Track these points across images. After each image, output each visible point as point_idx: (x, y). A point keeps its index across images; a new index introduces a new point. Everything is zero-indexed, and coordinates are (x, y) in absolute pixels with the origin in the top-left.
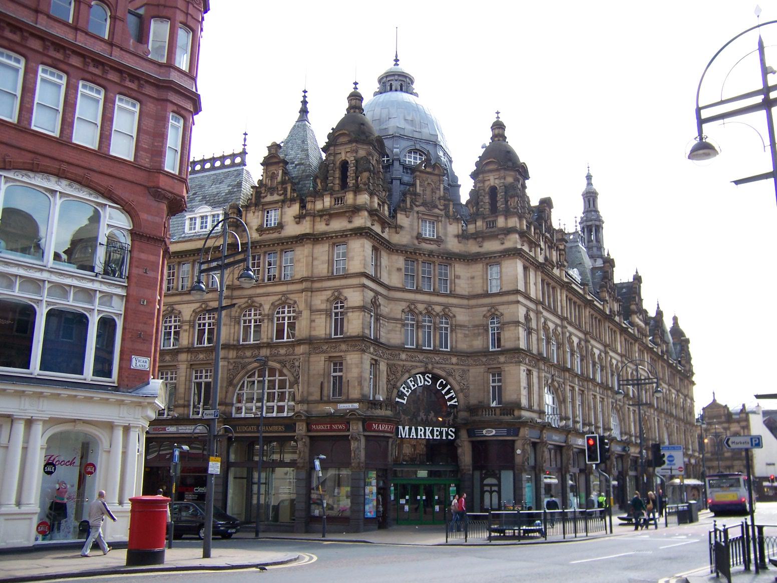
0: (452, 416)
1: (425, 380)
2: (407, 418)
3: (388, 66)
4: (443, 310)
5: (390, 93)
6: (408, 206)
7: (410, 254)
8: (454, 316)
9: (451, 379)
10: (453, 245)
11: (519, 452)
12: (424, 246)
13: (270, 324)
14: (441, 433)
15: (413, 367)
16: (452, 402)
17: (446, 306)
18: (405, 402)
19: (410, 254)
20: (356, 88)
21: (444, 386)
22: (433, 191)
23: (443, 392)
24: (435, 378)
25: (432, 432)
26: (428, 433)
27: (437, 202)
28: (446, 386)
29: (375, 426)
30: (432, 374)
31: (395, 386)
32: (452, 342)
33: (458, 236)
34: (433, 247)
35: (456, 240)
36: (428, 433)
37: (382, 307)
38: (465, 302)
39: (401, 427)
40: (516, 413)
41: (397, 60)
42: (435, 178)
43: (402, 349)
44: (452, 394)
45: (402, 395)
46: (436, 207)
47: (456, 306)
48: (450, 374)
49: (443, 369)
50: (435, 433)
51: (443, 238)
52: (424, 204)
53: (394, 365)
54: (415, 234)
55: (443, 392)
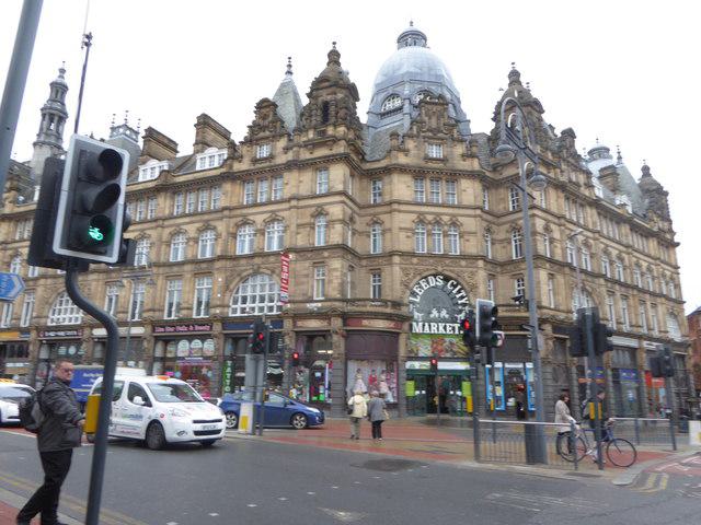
0: (463, 314)
3: (406, 28)
6: (415, 132)
12: (430, 164)
14: (454, 329)
16: (463, 301)
17: (454, 216)
18: (418, 300)
21: (455, 286)
23: (454, 292)
25: (445, 328)
26: (441, 328)
27: (442, 129)
36: (441, 328)
39: (414, 324)
42: (439, 108)
44: (463, 293)
45: (414, 294)
46: (442, 132)
50: (448, 328)
54: (422, 155)
55: (454, 292)
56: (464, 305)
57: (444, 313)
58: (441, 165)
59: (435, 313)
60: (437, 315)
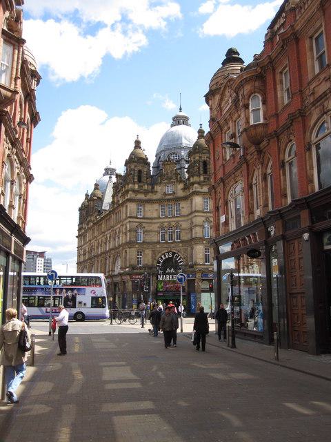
5: (182, 126)
7: (160, 201)
9: (179, 254)
10: (180, 194)
13: (124, 236)
17: (177, 222)
24: (174, 254)
34: (172, 197)
38: (186, 218)
43: (158, 243)
45: (159, 262)
47: (182, 221)
49: (176, 250)
56: (182, 265)
57: (172, 270)
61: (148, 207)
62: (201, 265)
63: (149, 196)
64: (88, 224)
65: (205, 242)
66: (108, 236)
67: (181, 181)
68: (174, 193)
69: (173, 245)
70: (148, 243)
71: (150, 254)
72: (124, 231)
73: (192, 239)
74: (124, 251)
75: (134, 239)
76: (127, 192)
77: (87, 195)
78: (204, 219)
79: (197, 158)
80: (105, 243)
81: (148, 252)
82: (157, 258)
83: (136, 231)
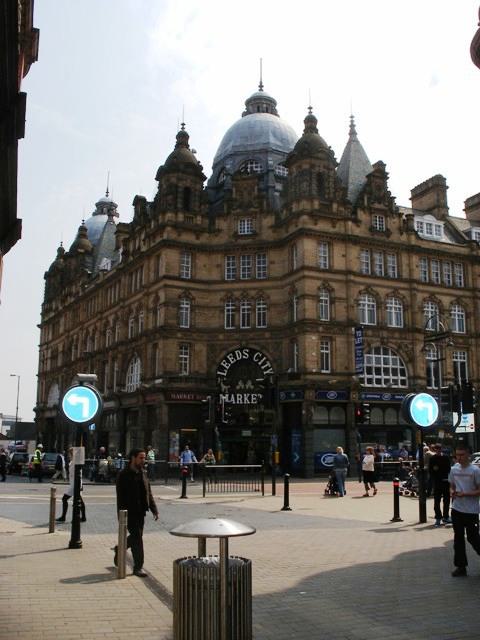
1: (243, 354)
2: (226, 387)
4: (257, 293)
6: (225, 211)
8: (269, 297)
9: (264, 352)
10: (267, 235)
11: (304, 412)
15: (231, 346)
16: (268, 372)
17: (261, 290)
19: (227, 250)
20: (183, 128)
21: (260, 358)
22: (250, 194)
25: (250, 398)
26: (246, 399)
28: (262, 357)
29: (173, 396)
30: (250, 349)
31: (214, 362)
32: (378, 317)
33: (271, 227)
34: (249, 241)
35: (270, 231)
37: (197, 299)
38: (279, 283)
40: (302, 377)
41: (261, 86)
43: (221, 330)
44: (268, 364)
45: (222, 369)
46: (252, 206)
48: (263, 347)
51: (258, 231)
52: (240, 207)
53: (213, 345)
54: (232, 233)
57: (249, 385)
58: (249, 241)
59: (240, 385)
60: (243, 387)
61: (202, 260)
62: (311, 373)
63: (204, 239)
64: (63, 301)
65: (321, 329)
66: (111, 319)
67: (269, 212)
68: (254, 234)
69: (251, 335)
70: (200, 331)
71: (204, 353)
72: (151, 306)
73: (291, 325)
74: (150, 346)
75: (173, 322)
76: (161, 228)
77: (61, 250)
78: (319, 283)
79: (306, 166)
80: (103, 334)
81: (201, 348)
82: (218, 360)
83: (178, 306)
